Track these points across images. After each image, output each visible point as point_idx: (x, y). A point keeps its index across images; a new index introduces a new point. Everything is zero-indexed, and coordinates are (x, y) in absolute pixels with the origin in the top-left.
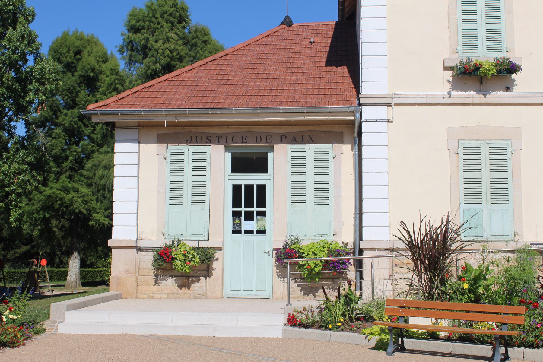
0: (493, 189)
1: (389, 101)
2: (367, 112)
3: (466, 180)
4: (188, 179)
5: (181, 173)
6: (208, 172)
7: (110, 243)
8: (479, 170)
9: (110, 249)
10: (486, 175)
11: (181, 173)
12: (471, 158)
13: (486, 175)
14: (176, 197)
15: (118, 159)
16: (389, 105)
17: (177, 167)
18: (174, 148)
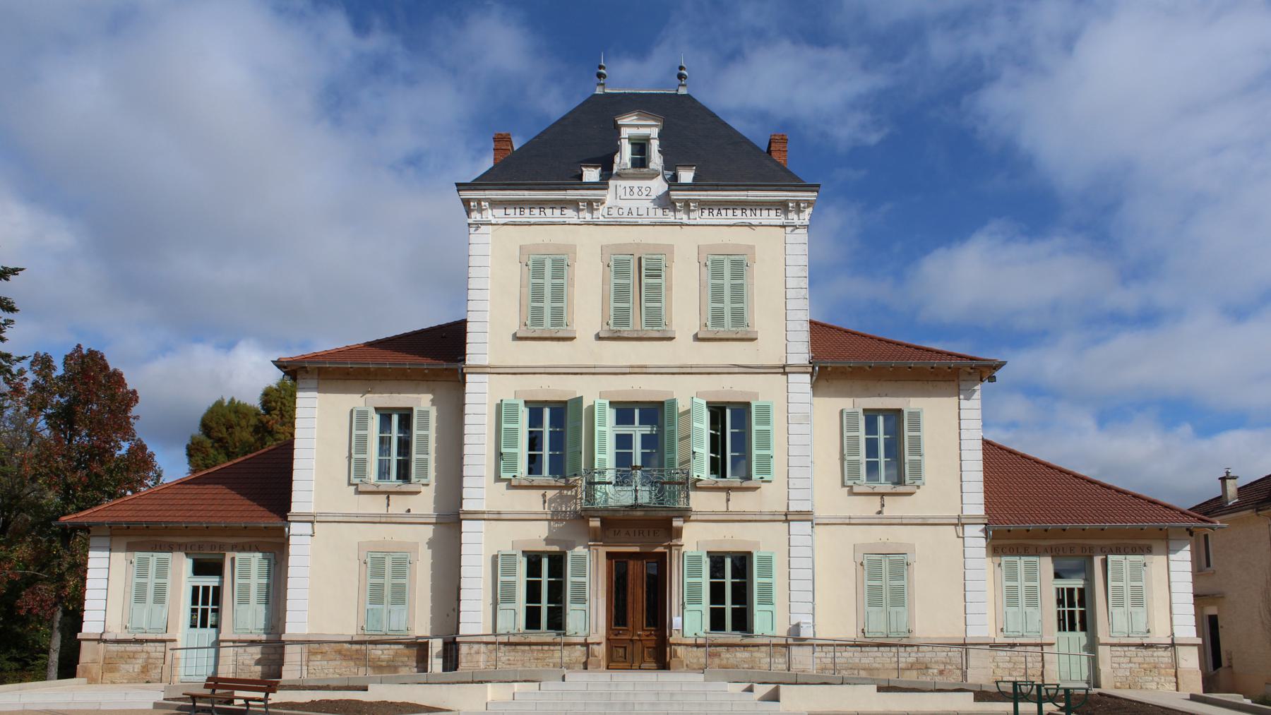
0: (394, 593)
1: (312, 519)
2: (295, 528)
3: (372, 585)
4: (151, 581)
5: (145, 576)
6: (169, 575)
7: (79, 636)
8: (383, 576)
9: (80, 641)
10: (388, 581)
11: (145, 576)
12: (377, 568)
13: (388, 581)
14: (140, 597)
15: (91, 564)
16: (312, 522)
17: (142, 571)
18: (138, 555)
